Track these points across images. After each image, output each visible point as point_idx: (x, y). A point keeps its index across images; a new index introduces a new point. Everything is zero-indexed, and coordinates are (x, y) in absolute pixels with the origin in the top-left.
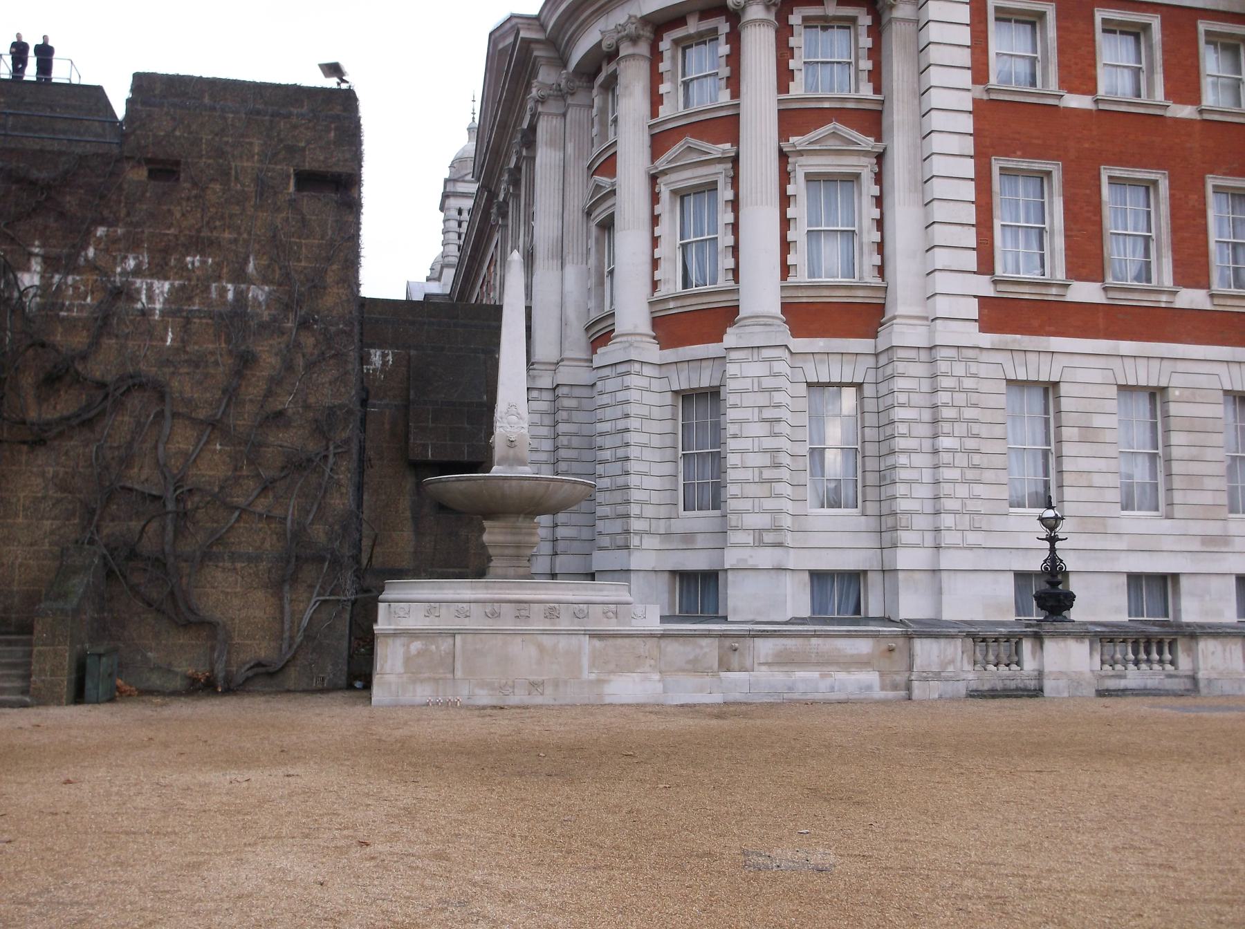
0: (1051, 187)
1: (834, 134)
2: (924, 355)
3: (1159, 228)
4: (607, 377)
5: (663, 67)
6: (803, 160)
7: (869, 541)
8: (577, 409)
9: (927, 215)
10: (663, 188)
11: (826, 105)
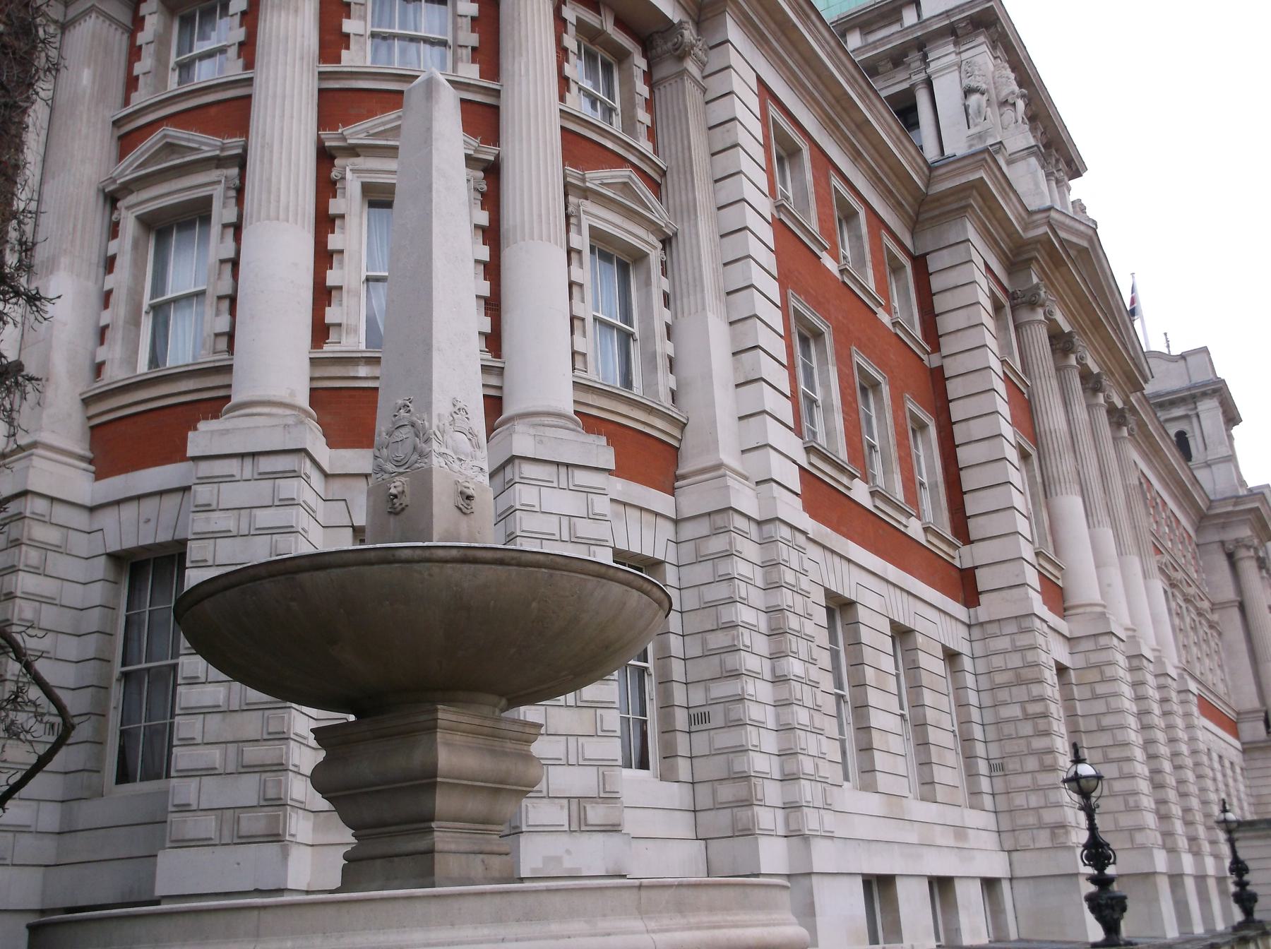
1: (626, 187)
2: (753, 530)
3: (883, 437)
4: (230, 478)
6: (587, 205)
7: (682, 825)
8: (57, 549)
9: (734, 338)
10: (349, 175)
11: (609, 145)
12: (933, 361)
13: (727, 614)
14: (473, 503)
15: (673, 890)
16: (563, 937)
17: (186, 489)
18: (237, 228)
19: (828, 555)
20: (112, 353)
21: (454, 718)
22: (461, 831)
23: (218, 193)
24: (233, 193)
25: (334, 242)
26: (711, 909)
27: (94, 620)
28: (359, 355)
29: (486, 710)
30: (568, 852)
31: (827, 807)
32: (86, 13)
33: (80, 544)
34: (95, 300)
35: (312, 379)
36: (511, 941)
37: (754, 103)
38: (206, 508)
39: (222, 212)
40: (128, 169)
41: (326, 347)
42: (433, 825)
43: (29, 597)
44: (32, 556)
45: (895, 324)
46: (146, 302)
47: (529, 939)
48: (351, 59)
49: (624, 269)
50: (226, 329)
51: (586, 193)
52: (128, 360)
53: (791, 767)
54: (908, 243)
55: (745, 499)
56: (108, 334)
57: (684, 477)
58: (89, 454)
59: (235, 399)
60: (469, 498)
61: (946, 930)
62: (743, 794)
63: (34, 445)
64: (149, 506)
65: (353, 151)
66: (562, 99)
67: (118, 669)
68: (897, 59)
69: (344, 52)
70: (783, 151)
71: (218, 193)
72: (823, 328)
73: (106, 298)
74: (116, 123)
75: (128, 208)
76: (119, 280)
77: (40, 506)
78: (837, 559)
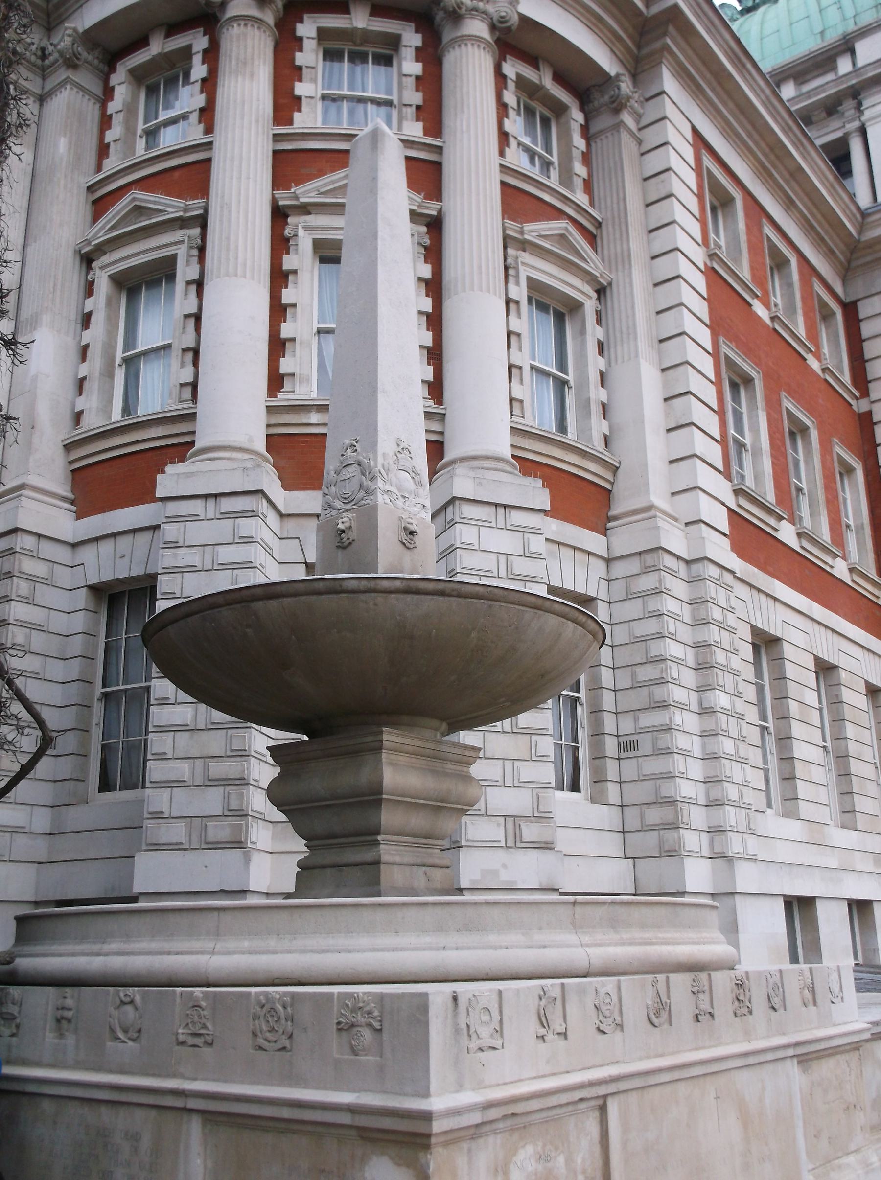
0: (752, 398)
3: (812, 481)
5: (300, 59)
6: (526, 257)
7: (612, 845)
8: (45, 581)
9: (665, 385)
10: (301, 232)
11: (547, 197)
12: (861, 406)
13: (656, 648)
14: (416, 538)
15: (606, 907)
16: (501, 947)
17: (156, 528)
18: (199, 284)
19: (755, 592)
20: (89, 402)
21: (398, 740)
22: (405, 844)
23: (182, 252)
24: (195, 252)
25: (287, 296)
26: (643, 926)
27: (76, 645)
28: (311, 403)
29: (428, 733)
30: (504, 866)
31: (751, 832)
32: (62, 85)
33: (64, 577)
34: (74, 354)
35: (268, 426)
36: (451, 949)
37: (689, 153)
38: (174, 545)
39: (186, 271)
40: (100, 232)
41: (281, 396)
42: (379, 838)
43: (20, 624)
44: (22, 587)
45: (825, 370)
46: (119, 355)
47: (469, 948)
48: (303, 121)
49: (560, 318)
50: (190, 379)
51: (524, 245)
52: (103, 410)
53: (715, 794)
54: (839, 289)
55: (675, 540)
56: (86, 385)
57: (616, 518)
58: (71, 496)
59: (198, 445)
60: (412, 533)
61: (864, 951)
62: (670, 818)
63: (23, 487)
64: (124, 543)
65: (305, 209)
66: (502, 154)
67: (99, 690)
68: (831, 108)
69: (296, 115)
70: (717, 201)
71: (182, 252)
72: (753, 374)
73: (84, 352)
74: (90, 189)
75: (102, 268)
76: (95, 335)
77: (29, 542)
78: (763, 598)
